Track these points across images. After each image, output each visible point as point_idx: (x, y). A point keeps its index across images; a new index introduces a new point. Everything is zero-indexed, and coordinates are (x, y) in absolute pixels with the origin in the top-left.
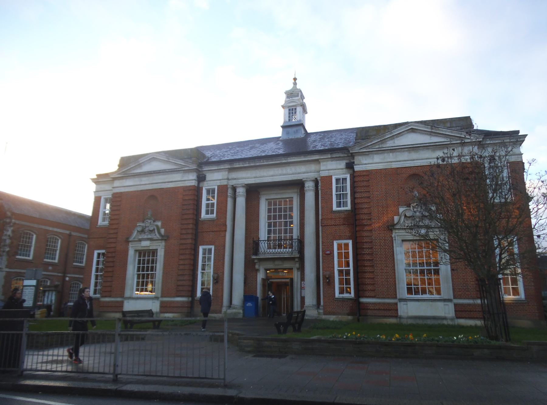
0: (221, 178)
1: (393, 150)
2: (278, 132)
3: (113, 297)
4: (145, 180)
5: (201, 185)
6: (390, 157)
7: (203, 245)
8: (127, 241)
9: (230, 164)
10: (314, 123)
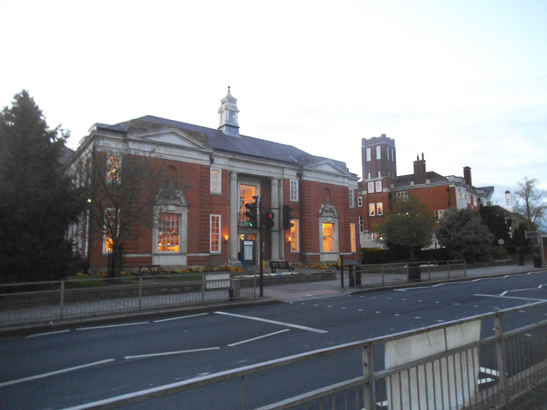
0: (223, 163)
1: (320, 172)
3: (139, 254)
8: (153, 203)
9: (234, 156)
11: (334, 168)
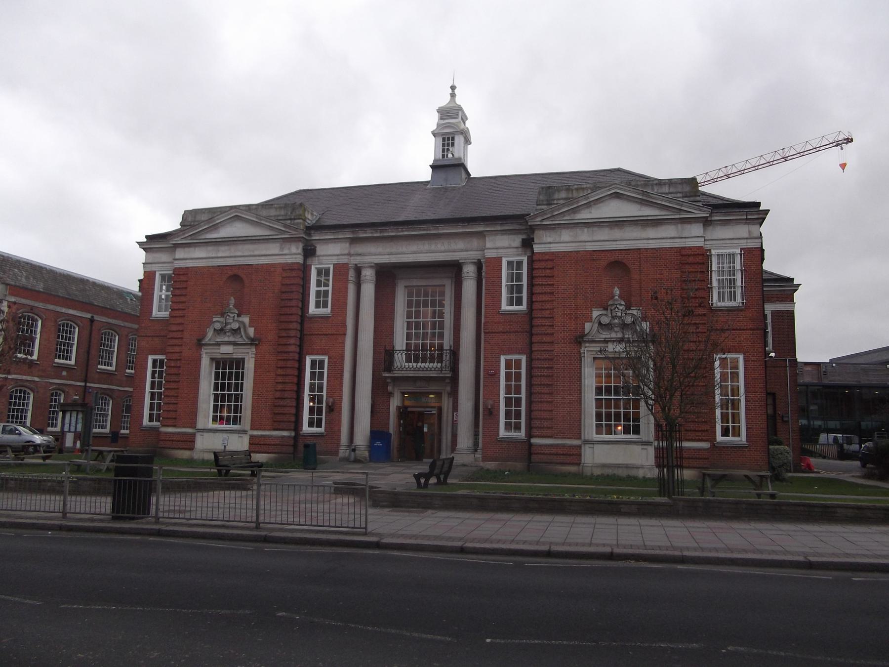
0: (338, 252)
1: (588, 224)
2: (425, 174)
4: (223, 251)
5: (309, 262)
6: (584, 235)
7: (312, 354)
8: (200, 344)
9: (353, 232)
10: (480, 162)
11: (644, 202)
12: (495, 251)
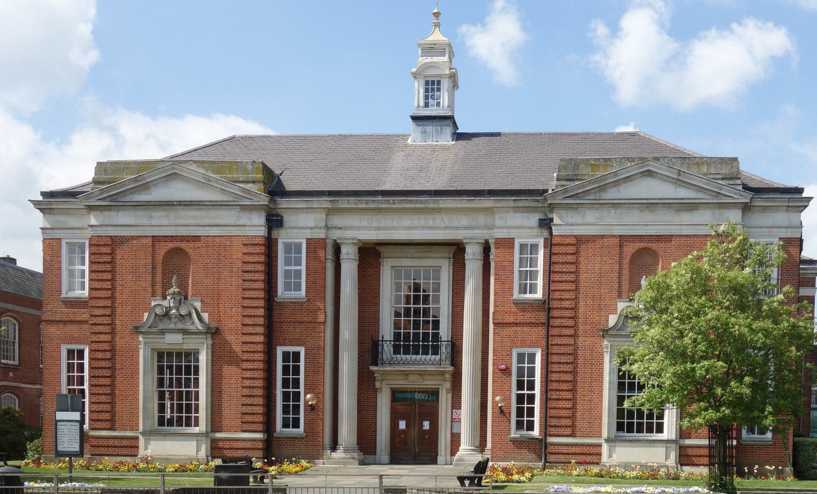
0: (312, 225)
1: (615, 205)
5: (274, 234)
7: (283, 345)
12: (506, 230)
